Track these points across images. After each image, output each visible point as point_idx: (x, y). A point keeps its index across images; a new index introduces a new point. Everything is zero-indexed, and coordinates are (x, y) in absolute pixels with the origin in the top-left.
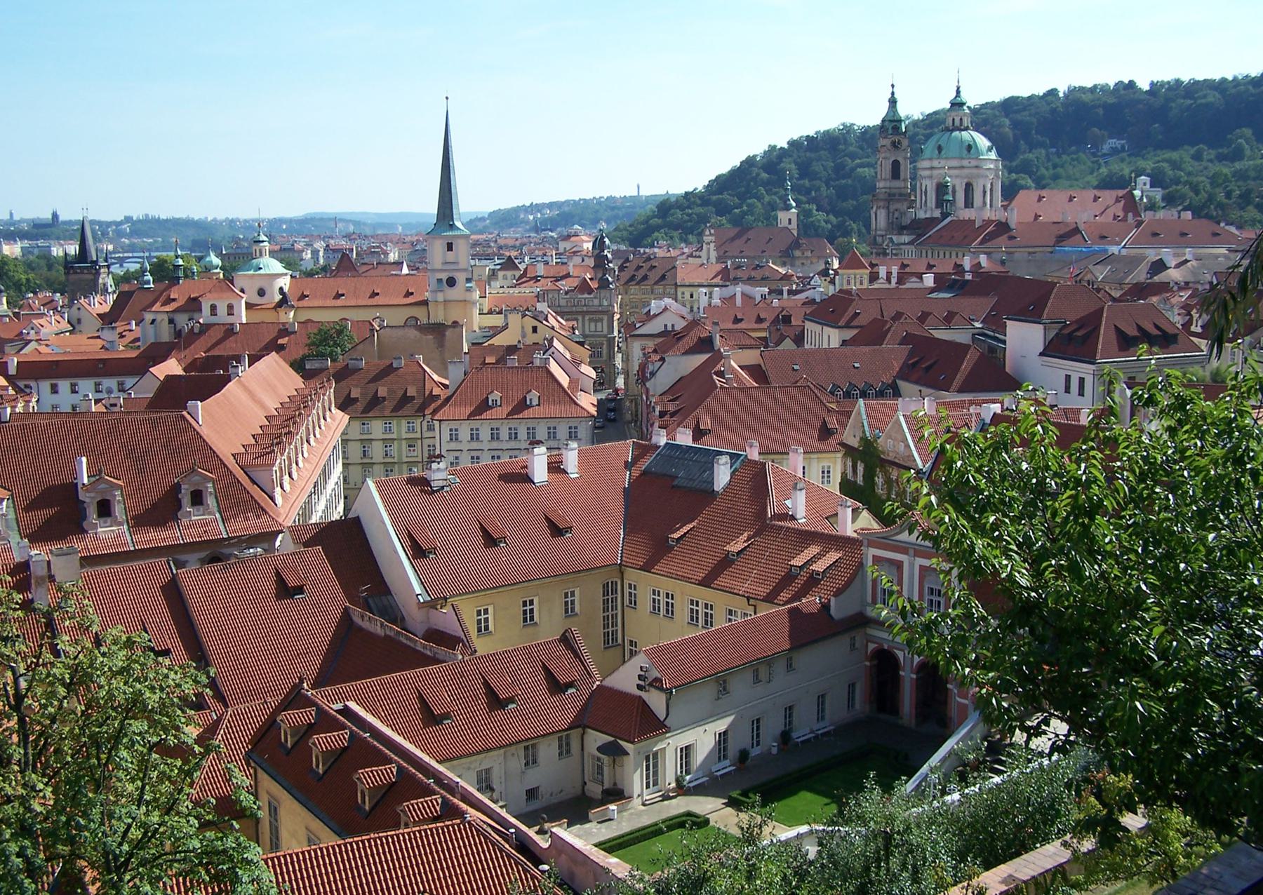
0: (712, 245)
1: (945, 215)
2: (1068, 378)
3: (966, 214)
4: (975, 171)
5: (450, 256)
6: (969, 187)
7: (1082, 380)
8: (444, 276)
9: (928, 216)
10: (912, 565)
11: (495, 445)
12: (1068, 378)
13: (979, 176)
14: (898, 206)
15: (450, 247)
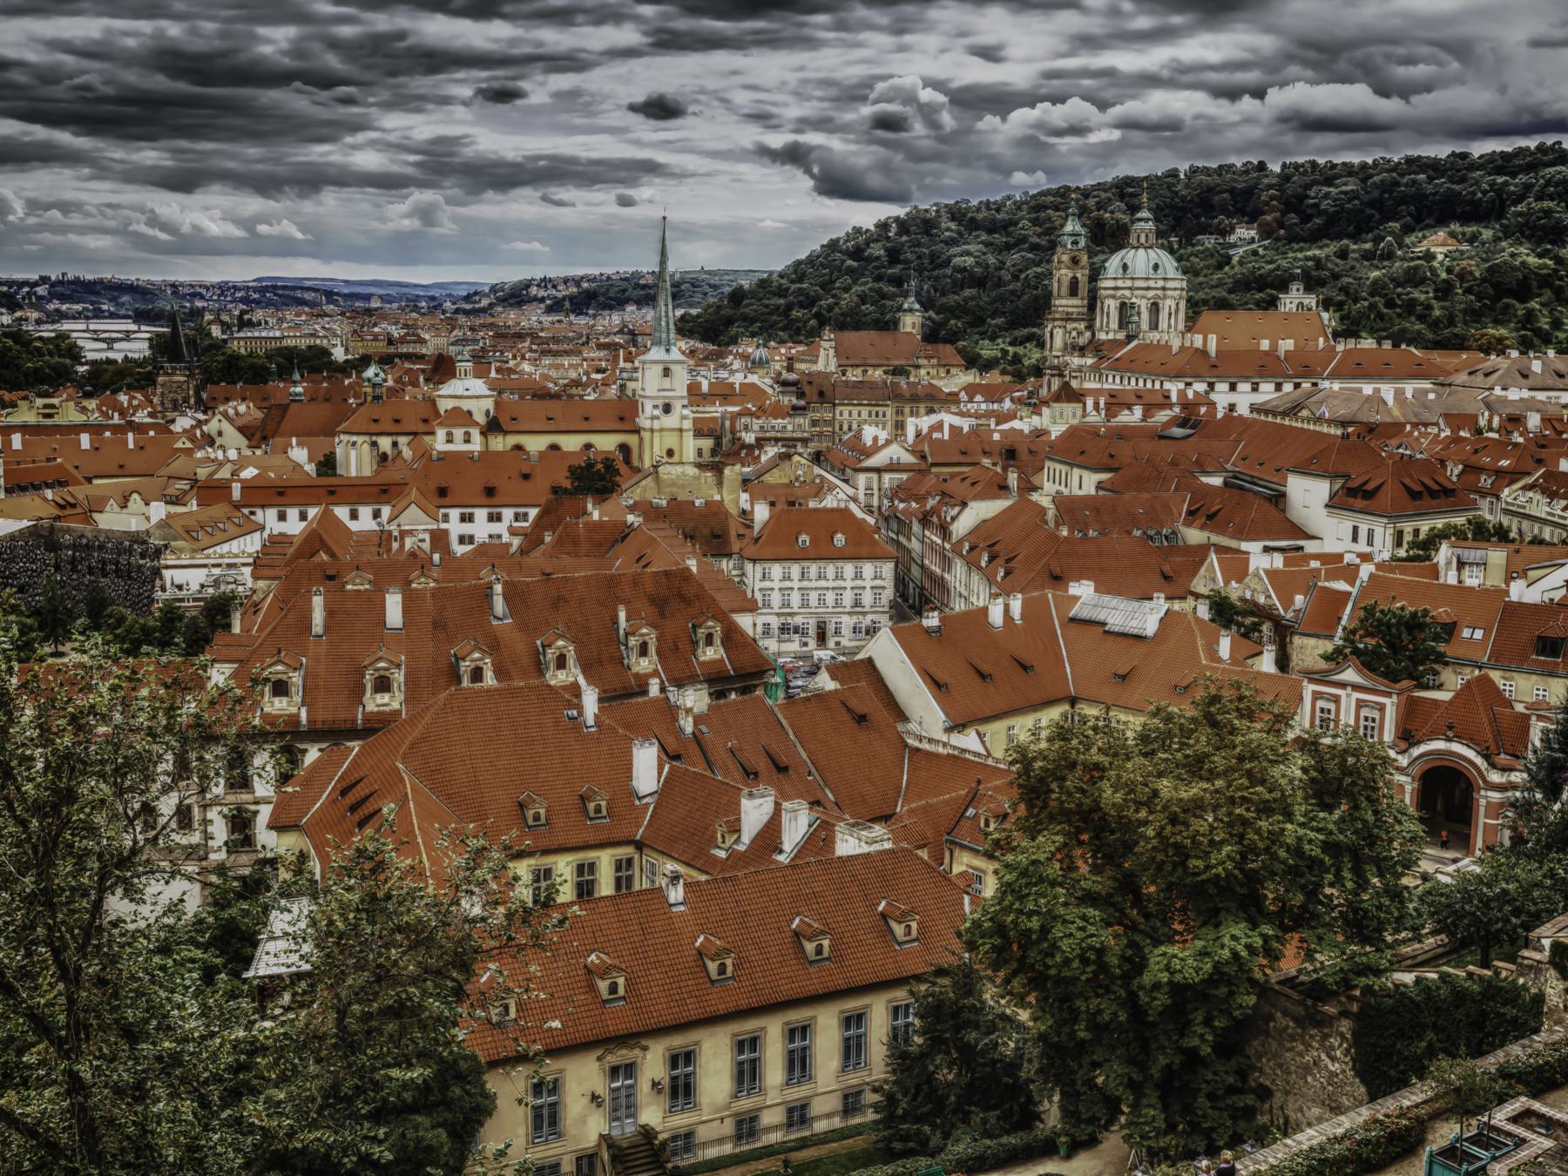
0: (832, 352)
1: (1130, 338)
2: (1355, 529)
3: (1154, 337)
4: (1160, 293)
5: (667, 383)
6: (1155, 308)
7: (1371, 533)
8: (660, 402)
9: (1111, 336)
10: (1348, 696)
11: (805, 584)
12: (1355, 529)
13: (1165, 297)
14: (1075, 325)
15: (667, 372)
